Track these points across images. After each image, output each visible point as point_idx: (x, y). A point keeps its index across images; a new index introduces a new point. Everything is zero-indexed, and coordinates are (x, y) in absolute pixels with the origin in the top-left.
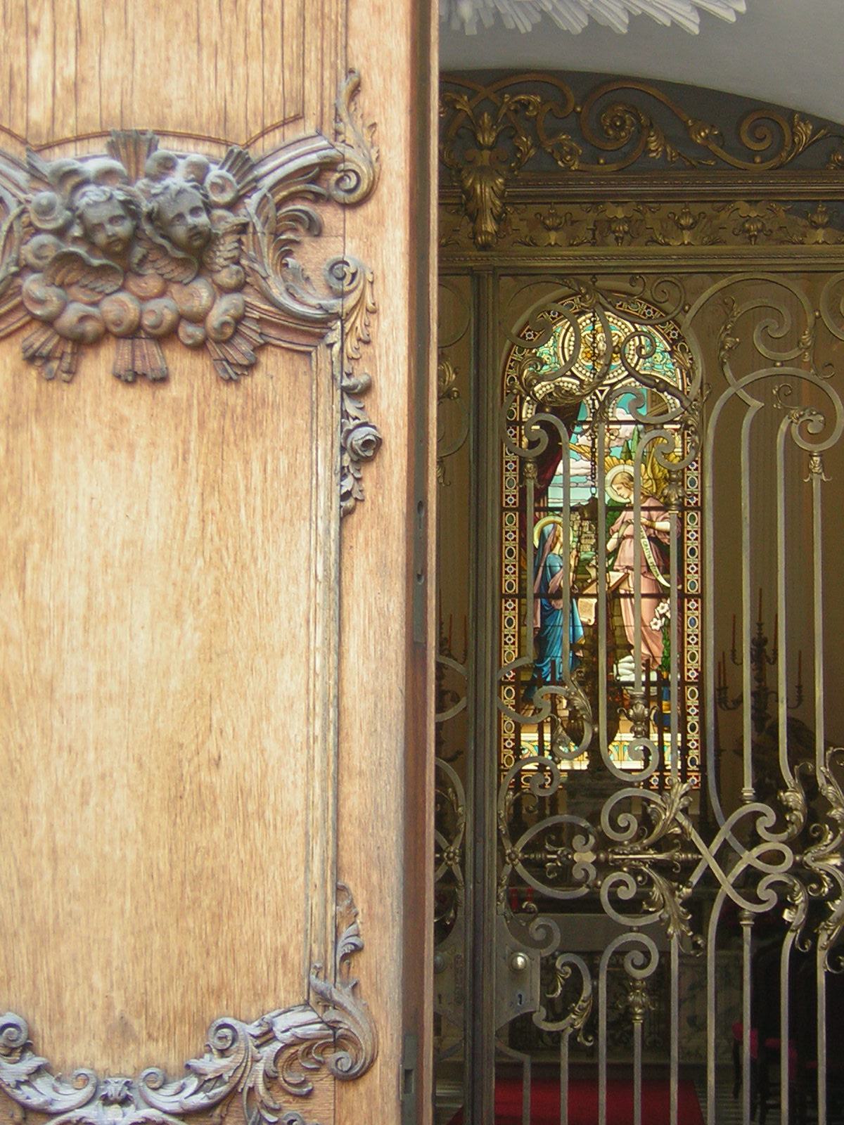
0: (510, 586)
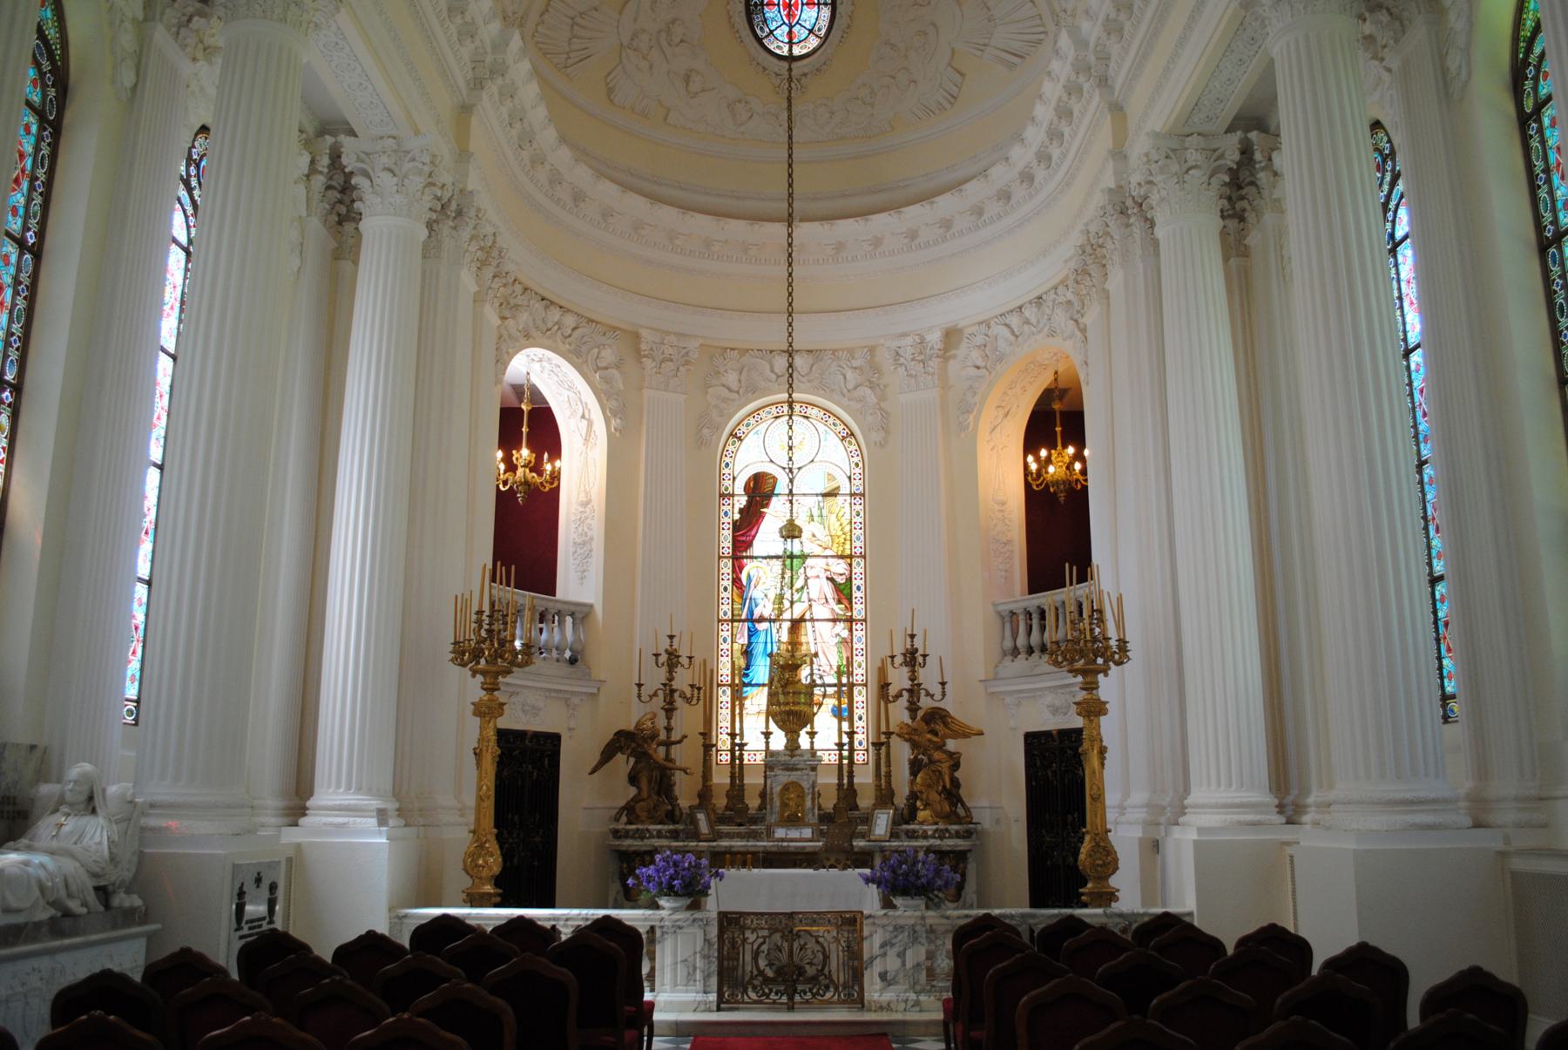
0: (725, 614)
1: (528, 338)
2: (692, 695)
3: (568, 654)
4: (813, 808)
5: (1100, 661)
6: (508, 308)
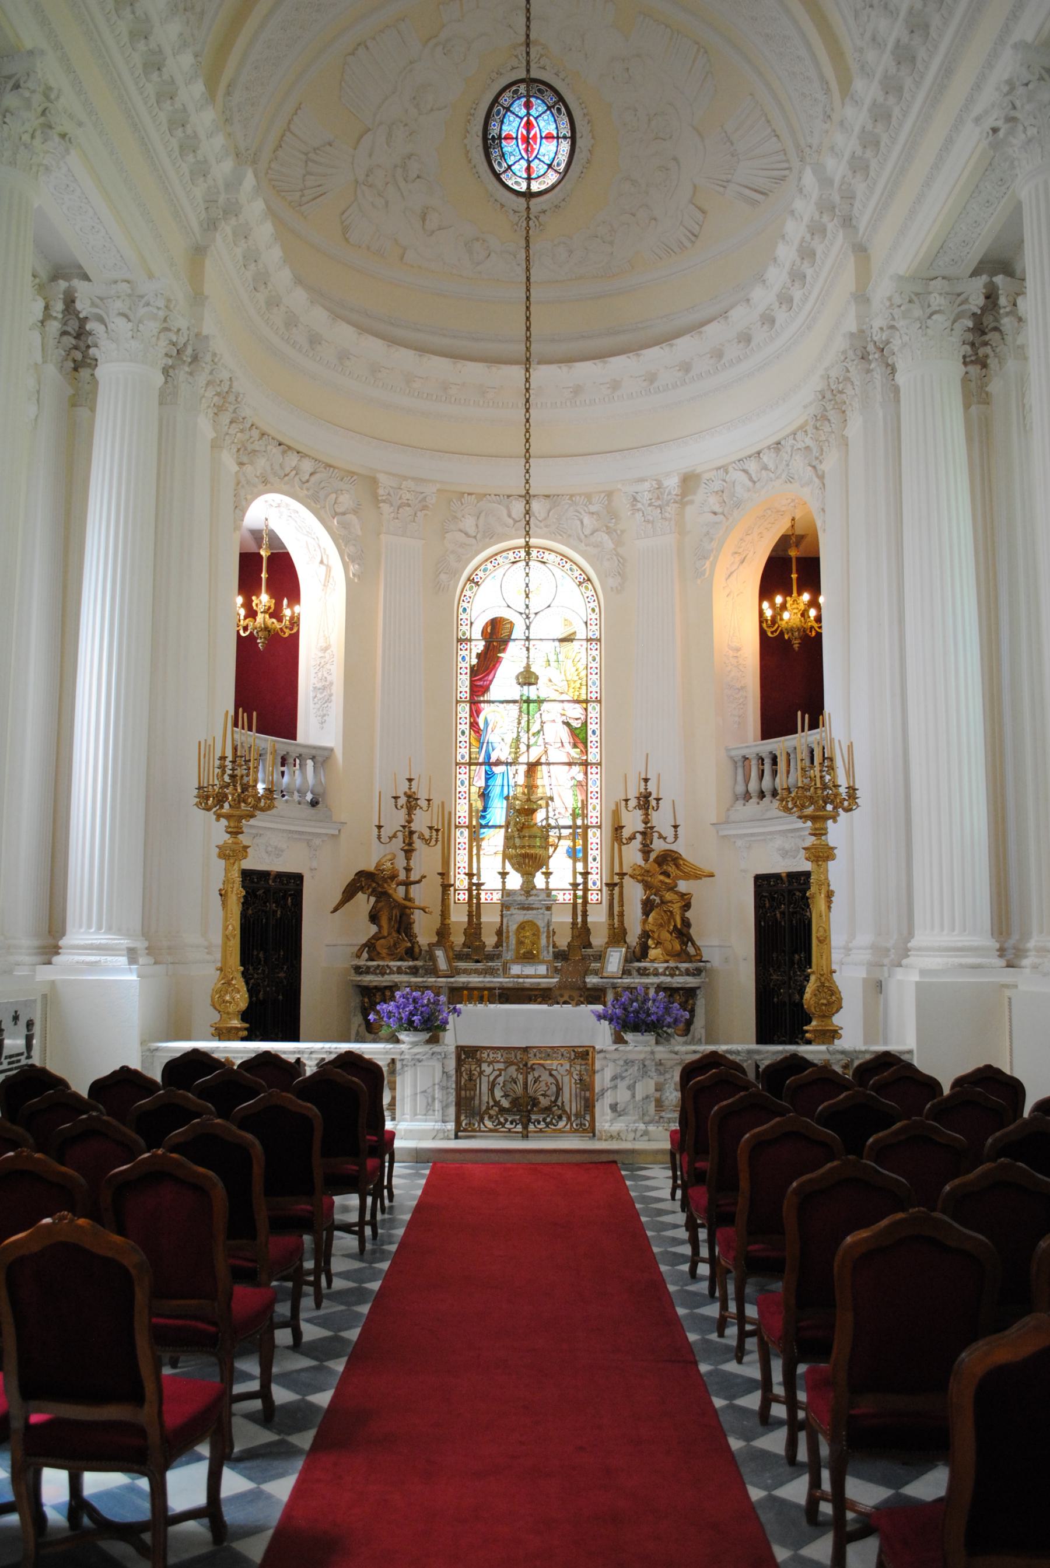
0: (463, 757)
1: (266, 484)
2: (431, 836)
3: (309, 797)
4: (548, 947)
5: (829, 807)
6: (245, 454)
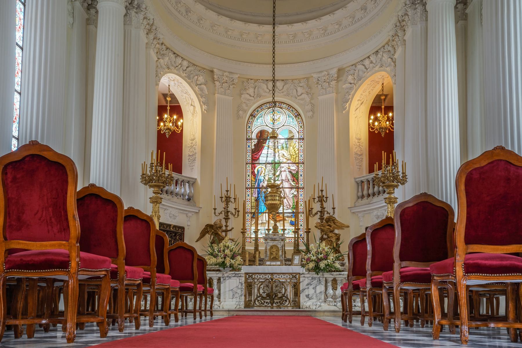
0: (249, 185)
